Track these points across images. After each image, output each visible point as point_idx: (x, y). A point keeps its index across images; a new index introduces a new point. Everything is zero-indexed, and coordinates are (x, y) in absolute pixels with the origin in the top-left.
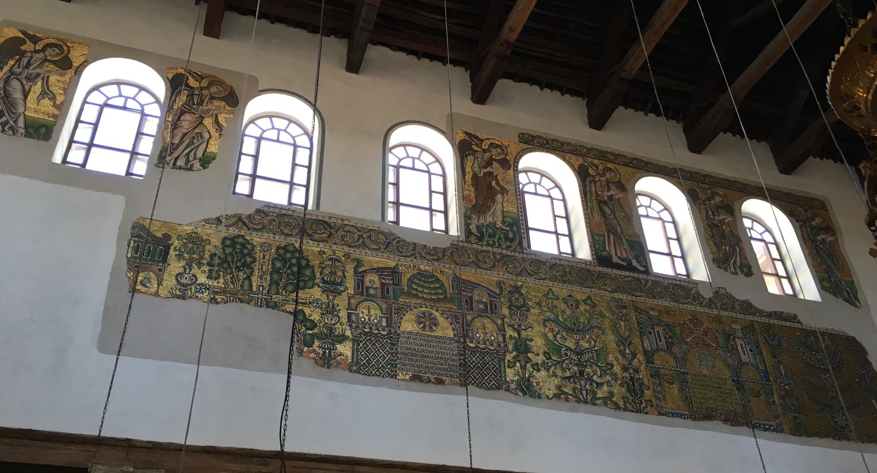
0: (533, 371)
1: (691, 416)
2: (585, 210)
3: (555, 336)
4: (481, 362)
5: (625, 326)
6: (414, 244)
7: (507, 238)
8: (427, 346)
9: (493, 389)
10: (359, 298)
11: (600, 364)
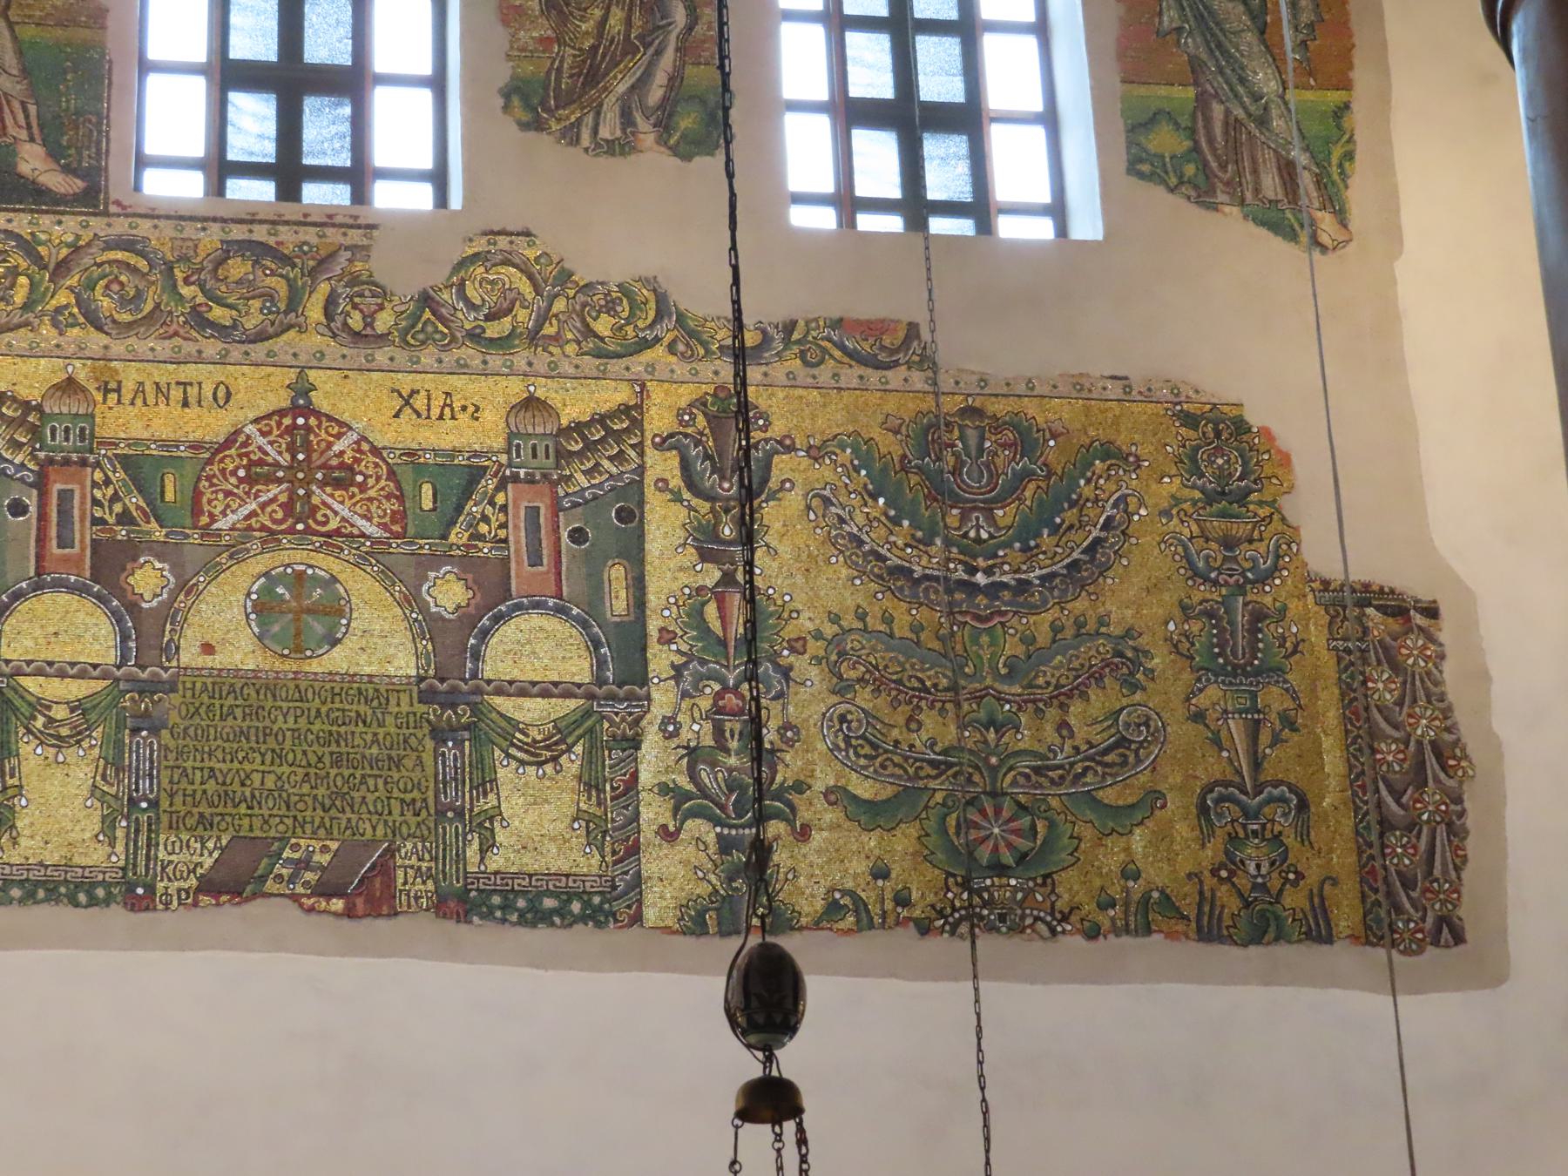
1: (131, 888)
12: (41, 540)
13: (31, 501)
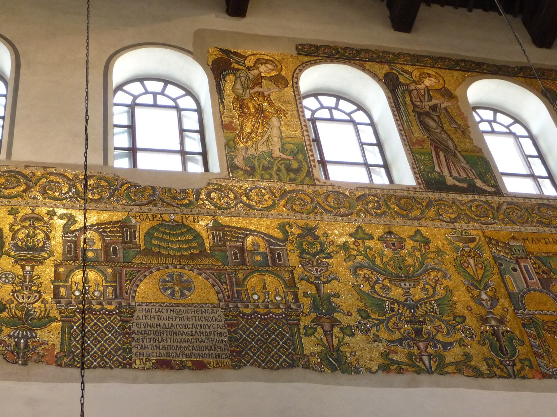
0: (343, 337)
2: (399, 125)
3: (373, 287)
4: (262, 332)
5: (476, 265)
6: (153, 188)
7: (289, 170)
8: (177, 319)
9: (283, 368)
10: (71, 264)
11: (444, 318)
12: (525, 278)
13: (517, 267)
